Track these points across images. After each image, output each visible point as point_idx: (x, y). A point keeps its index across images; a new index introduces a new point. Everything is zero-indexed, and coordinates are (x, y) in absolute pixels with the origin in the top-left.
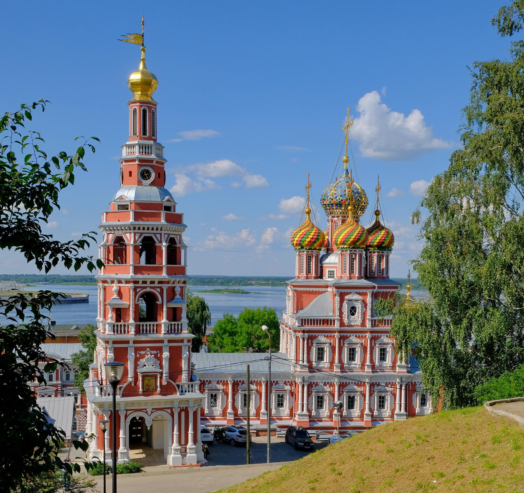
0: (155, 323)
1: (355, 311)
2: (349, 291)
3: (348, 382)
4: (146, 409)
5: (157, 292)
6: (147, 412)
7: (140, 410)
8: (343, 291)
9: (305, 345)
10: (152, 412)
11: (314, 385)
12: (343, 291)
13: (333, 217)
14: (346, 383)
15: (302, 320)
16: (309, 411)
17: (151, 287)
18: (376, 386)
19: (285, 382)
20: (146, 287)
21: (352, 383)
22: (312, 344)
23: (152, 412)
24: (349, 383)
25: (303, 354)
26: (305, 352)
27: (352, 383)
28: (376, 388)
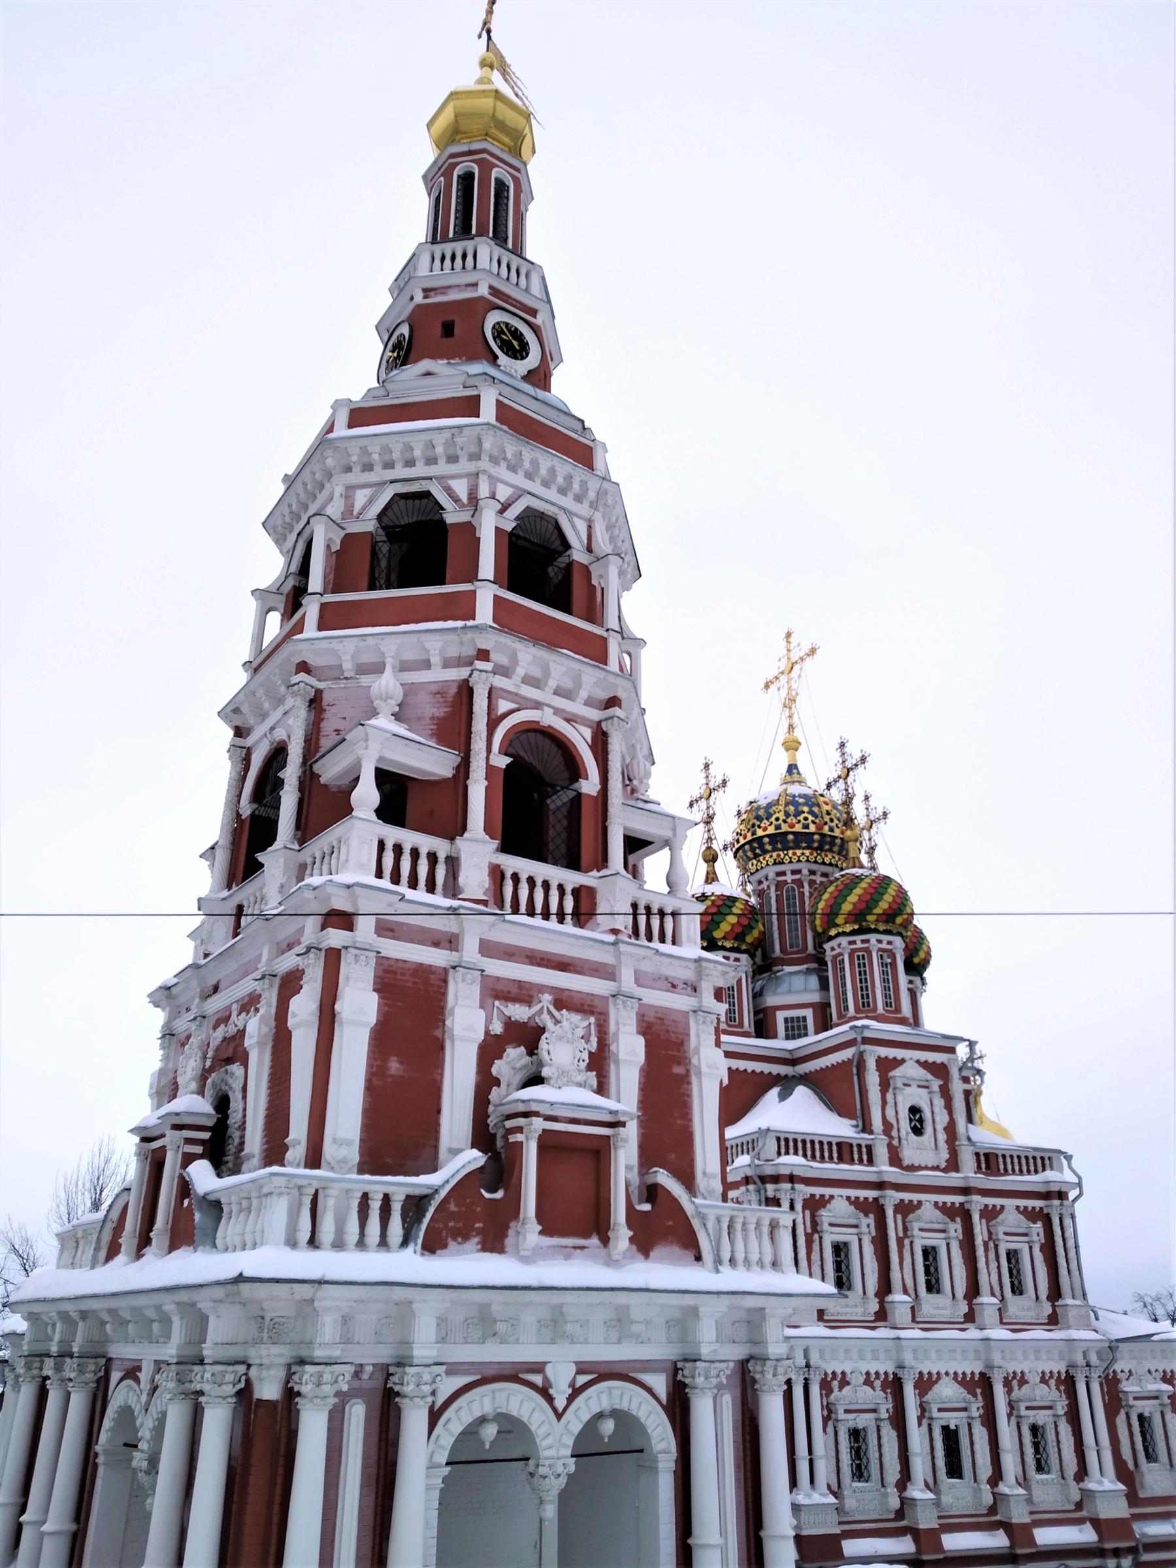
0: (572, 879)
1: (921, 1121)
3: (934, 1372)
4: (539, 1368)
5: (580, 739)
6: (544, 1392)
7: (512, 1374)
10: (576, 1392)
11: (835, 1384)
13: (783, 873)
14: (929, 1373)
15: (778, 1139)
17: (557, 711)
20: (537, 705)
21: (947, 1374)
22: (815, 1224)
23: (576, 1392)
24: (938, 1373)
27: (947, 1374)
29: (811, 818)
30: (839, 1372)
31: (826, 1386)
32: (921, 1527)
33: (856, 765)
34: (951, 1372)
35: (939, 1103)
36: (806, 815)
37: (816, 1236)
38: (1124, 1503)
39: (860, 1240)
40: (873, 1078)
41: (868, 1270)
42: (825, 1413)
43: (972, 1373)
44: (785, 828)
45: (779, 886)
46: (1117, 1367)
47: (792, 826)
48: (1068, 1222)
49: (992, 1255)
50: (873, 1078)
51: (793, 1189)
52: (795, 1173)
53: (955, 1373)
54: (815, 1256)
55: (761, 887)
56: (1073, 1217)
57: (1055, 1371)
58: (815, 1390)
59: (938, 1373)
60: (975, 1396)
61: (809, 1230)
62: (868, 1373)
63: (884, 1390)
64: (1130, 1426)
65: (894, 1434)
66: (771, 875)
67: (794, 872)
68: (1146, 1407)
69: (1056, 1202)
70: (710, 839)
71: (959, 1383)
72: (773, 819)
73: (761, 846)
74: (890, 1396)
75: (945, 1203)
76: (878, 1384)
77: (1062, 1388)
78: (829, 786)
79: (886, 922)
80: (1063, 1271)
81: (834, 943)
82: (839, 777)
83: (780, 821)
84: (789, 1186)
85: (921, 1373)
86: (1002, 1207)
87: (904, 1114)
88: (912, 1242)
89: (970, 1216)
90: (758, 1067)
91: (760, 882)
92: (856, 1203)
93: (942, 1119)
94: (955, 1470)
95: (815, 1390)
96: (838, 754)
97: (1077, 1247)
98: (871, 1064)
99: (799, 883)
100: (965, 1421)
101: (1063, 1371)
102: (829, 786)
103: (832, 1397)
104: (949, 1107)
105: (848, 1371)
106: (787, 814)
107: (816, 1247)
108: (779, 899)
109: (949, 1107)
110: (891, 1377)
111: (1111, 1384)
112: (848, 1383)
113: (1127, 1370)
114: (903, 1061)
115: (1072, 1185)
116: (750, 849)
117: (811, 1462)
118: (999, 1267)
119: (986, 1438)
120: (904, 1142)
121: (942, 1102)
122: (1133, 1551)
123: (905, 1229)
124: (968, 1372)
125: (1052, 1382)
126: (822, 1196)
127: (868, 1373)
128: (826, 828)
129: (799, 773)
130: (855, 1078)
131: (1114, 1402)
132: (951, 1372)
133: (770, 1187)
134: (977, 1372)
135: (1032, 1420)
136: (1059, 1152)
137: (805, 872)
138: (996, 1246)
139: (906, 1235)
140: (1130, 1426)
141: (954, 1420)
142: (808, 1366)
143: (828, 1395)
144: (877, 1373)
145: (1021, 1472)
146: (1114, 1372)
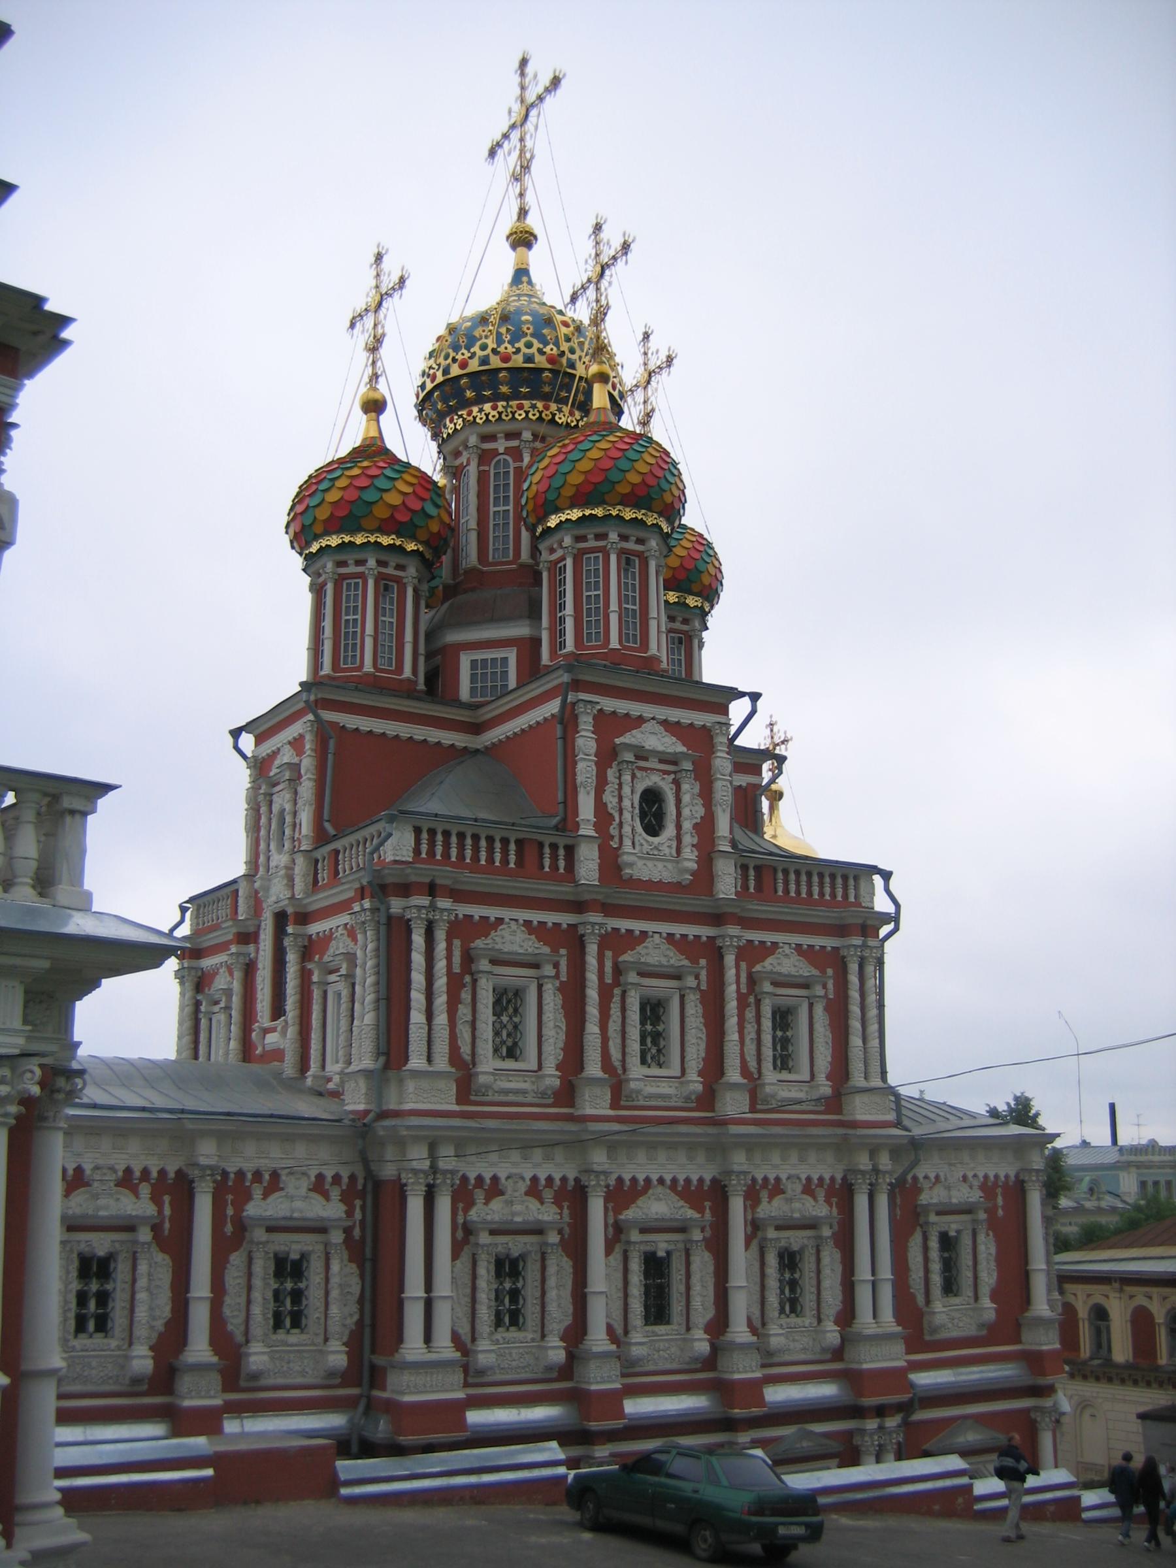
2: (635, 708)
3: (641, 1177)
8: (609, 704)
9: (441, 965)
12: (609, 704)
13: (492, 438)
14: (634, 1180)
15: (418, 831)
16: (456, 1338)
18: (764, 1195)
19: (320, 1177)
21: (661, 1181)
22: (468, 959)
24: (648, 1180)
25: (430, 1015)
26: (441, 1000)
27: (661, 1181)
28: (770, 1208)
29: (537, 345)
30: (487, 1177)
31: (463, 1195)
32: (594, 1387)
33: (614, 258)
34: (668, 1178)
35: (690, 788)
36: (529, 338)
37: (468, 979)
38: (899, 1348)
39: (540, 987)
40: (586, 742)
41: (549, 1032)
42: (460, 1234)
43: (701, 1180)
44: (495, 362)
45: (485, 457)
46: (920, 1172)
47: (506, 358)
48: (870, 969)
49: (750, 1014)
50: (586, 742)
51: (433, 907)
52: (439, 881)
53: (674, 1181)
54: (464, 1011)
55: (457, 463)
56: (880, 963)
57: (827, 1177)
58: (444, 1206)
59: (648, 1180)
60: (701, 1210)
61: (457, 969)
62: (535, 1179)
63: (557, 1202)
64: (926, 1249)
65: (567, 1264)
66: (473, 440)
67: (509, 436)
68: (953, 1225)
69: (857, 941)
70: (375, 377)
71: (677, 1193)
72: (476, 348)
73: (459, 393)
74: (566, 1211)
75: (684, 936)
76: (548, 1195)
77: (834, 1200)
78: (574, 298)
79: (637, 506)
80: (856, 1041)
81: (552, 541)
82: (589, 280)
83: (489, 351)
84: (425, 901)
85: (620, 1180)
86: (775, 945)
87: (632, 801)
88: (624, 992)
89: (721, 957)
90: (420, 732)
91: (457, 454)
92: (537, 930)
93: (693, 811)
94: (657, 1312)
95: (444, 1206)
96: (591, 243)
97: (881, 1006)
98: (586, 723)
99: (516, 453)
100: (681, 1246)
101: (839, 1177)
102: (574, 298)
103: (473, 1214)
104: (707, 795)
105: (502, 1175)
106: (500, 341)
107: (466, 995)
108: (482, 478)
109: (707, 795)
110: (571, 1183)
111: (905, 1193)
112: (502, 1193)
113: (932, 1176)
114: (640, 720)
115: (885, 918)
116: (441, 401)
117: (429, 1304)
118: (759, 1032)
119: (711, 1269)
120: (627, 842)
121: (697, 790)
122: (904, 1408)
123: (618, 971)
124: (695, 1178)
125: (821, 1194)
126: (484, 919)
127: (535, 1179)
128: (564, 361)
129: (530, 283)
130: (560, 742)
131: (909, 1216)
132: (668, 1178)
133: (396, 905)
134: (708, 1177)
135: (783, 1243)
136: (875, 870)
137: (527, 435)
138: (758, 1002)
139: (616, 983)
140: (926, 1249)
141: (662, 1244)
142: (434, 1169)
143: (466, 1211)
144: (550, 1179)
145: (757, 1313)
146: (915, 1178)
